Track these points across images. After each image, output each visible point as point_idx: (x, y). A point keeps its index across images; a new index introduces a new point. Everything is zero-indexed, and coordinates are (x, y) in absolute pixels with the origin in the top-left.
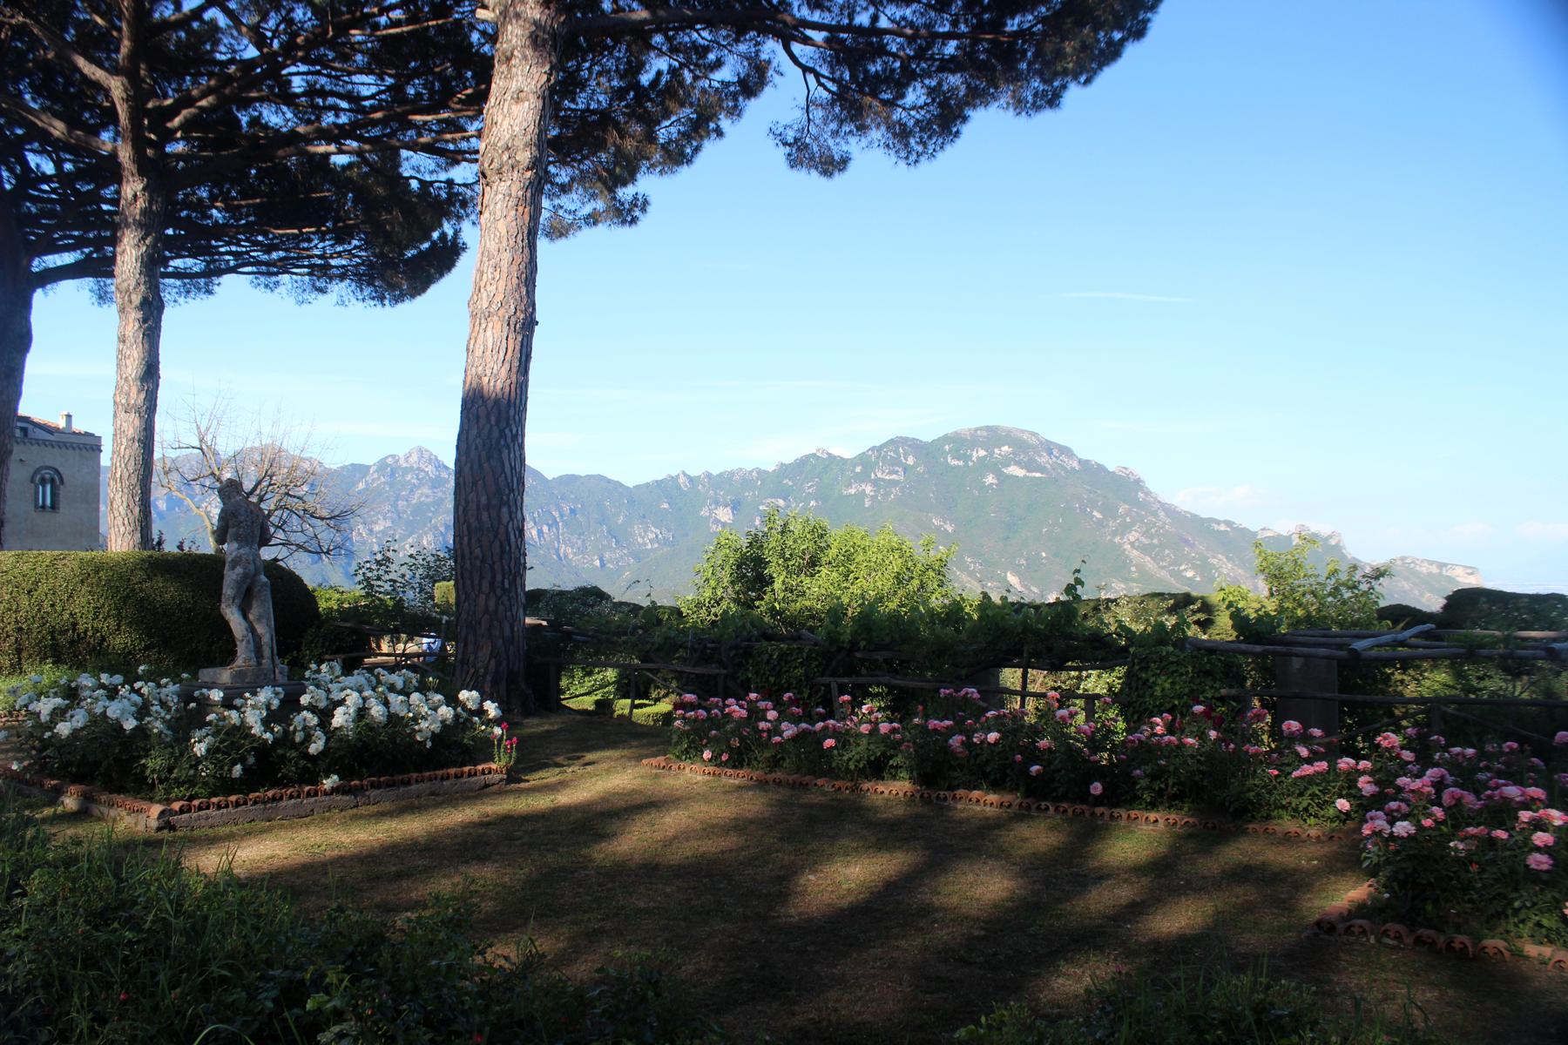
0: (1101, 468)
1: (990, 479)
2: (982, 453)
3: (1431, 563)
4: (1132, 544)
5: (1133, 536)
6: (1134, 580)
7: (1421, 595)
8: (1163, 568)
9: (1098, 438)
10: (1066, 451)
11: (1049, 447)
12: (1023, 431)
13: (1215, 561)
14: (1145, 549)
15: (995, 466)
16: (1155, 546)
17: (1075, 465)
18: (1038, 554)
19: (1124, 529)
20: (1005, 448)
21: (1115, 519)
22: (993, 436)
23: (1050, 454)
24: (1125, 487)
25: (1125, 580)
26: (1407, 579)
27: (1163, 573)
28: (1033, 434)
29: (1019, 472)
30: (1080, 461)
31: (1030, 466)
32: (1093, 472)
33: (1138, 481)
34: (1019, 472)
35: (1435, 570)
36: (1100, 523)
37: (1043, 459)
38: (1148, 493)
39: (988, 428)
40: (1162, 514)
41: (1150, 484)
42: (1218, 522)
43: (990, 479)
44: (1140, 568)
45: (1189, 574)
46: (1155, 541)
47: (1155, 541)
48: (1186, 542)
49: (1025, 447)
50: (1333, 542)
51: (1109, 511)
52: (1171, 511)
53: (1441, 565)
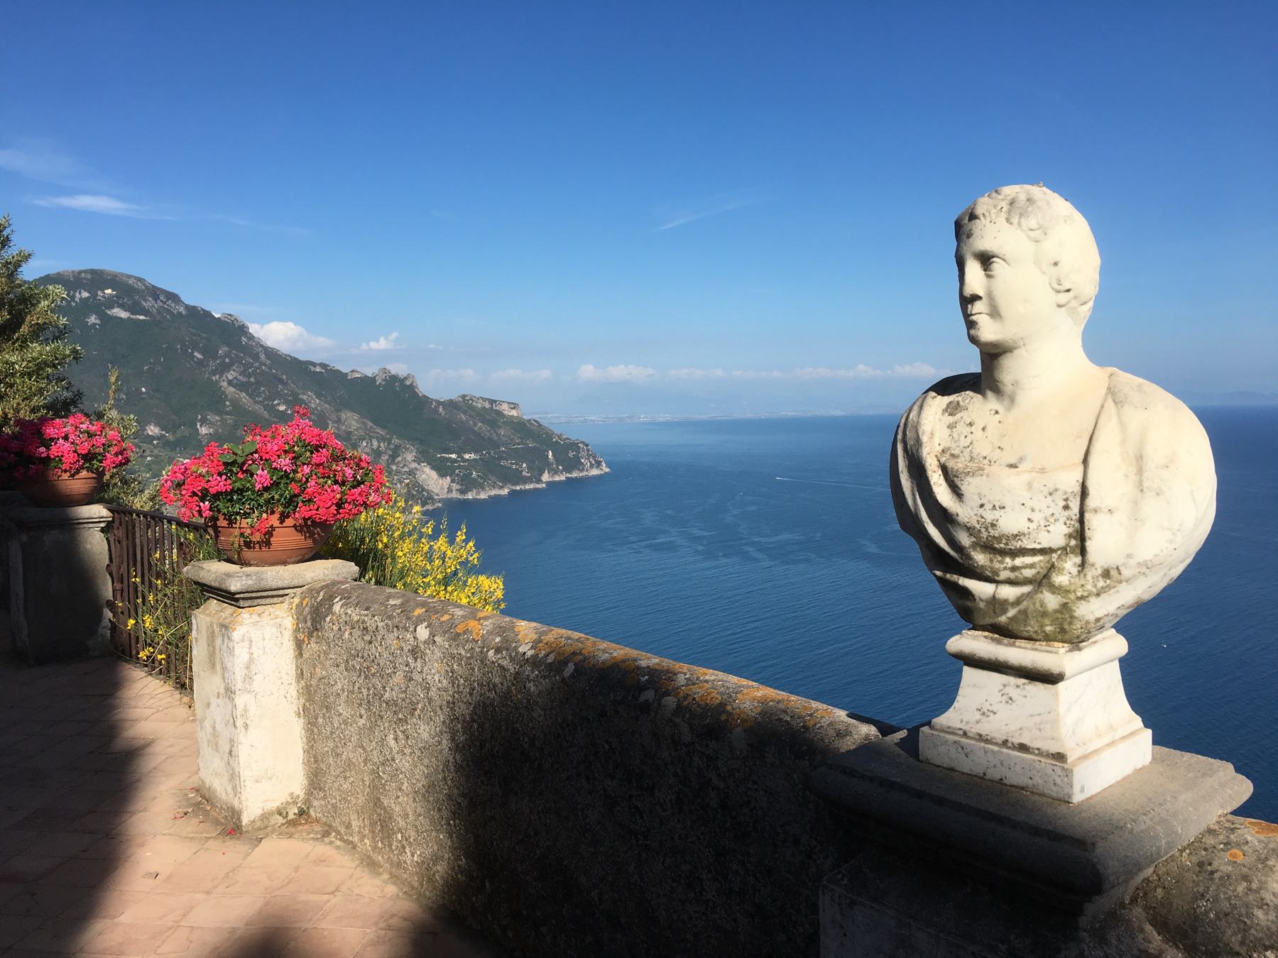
0: (208, 314)
1: (93, 319)
2: (85, 295)
3: (484, 400)
4: (230, 383)
5: (231, 375)
6: (227, 413)
7: (475, 424)
8: (258, 402)
9: (203, 285)
10: (174, 297)
11: (155, 292)
12: (129, 277)
13: (305, 397)
14: (241, 386)
15: (99, 307)
16: (252, 384)
17: (182, 309)
18: (138, 390)
19: (223, 368)
20: (109, 291)
21: (215, 358)
22: (97, 279)
23: (156, 298)
24: (232, 332)
25: (220, 413)
26: (465, 413)
27: (257, 407)
28: (140, 279)
29: (124, 315)
30: (187, 307)
31: (134, 308)
32: (199, 317)
33: (243, 329)
34: (124, 315)
35: (487, 405)
36: (200, 362)
37: (149, 303)
38: (251, 337)
39: (93, 272)
40: (263, 357)
41: (254, 329)
42: (314, 365)
43: (93, 319)
44: (235, 403)
45: (282, 408)
46: (252, 379)
47: (252, 379)
48: (281, 381)
49: (130, 292)
50: (408, 383)
51: (210, 353)
52: (271, 354)
53: (492, 402)
